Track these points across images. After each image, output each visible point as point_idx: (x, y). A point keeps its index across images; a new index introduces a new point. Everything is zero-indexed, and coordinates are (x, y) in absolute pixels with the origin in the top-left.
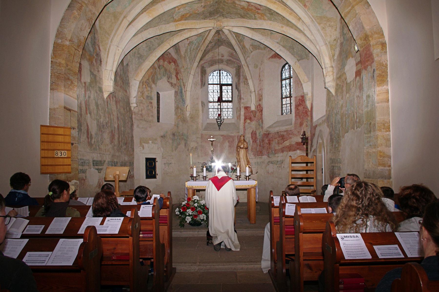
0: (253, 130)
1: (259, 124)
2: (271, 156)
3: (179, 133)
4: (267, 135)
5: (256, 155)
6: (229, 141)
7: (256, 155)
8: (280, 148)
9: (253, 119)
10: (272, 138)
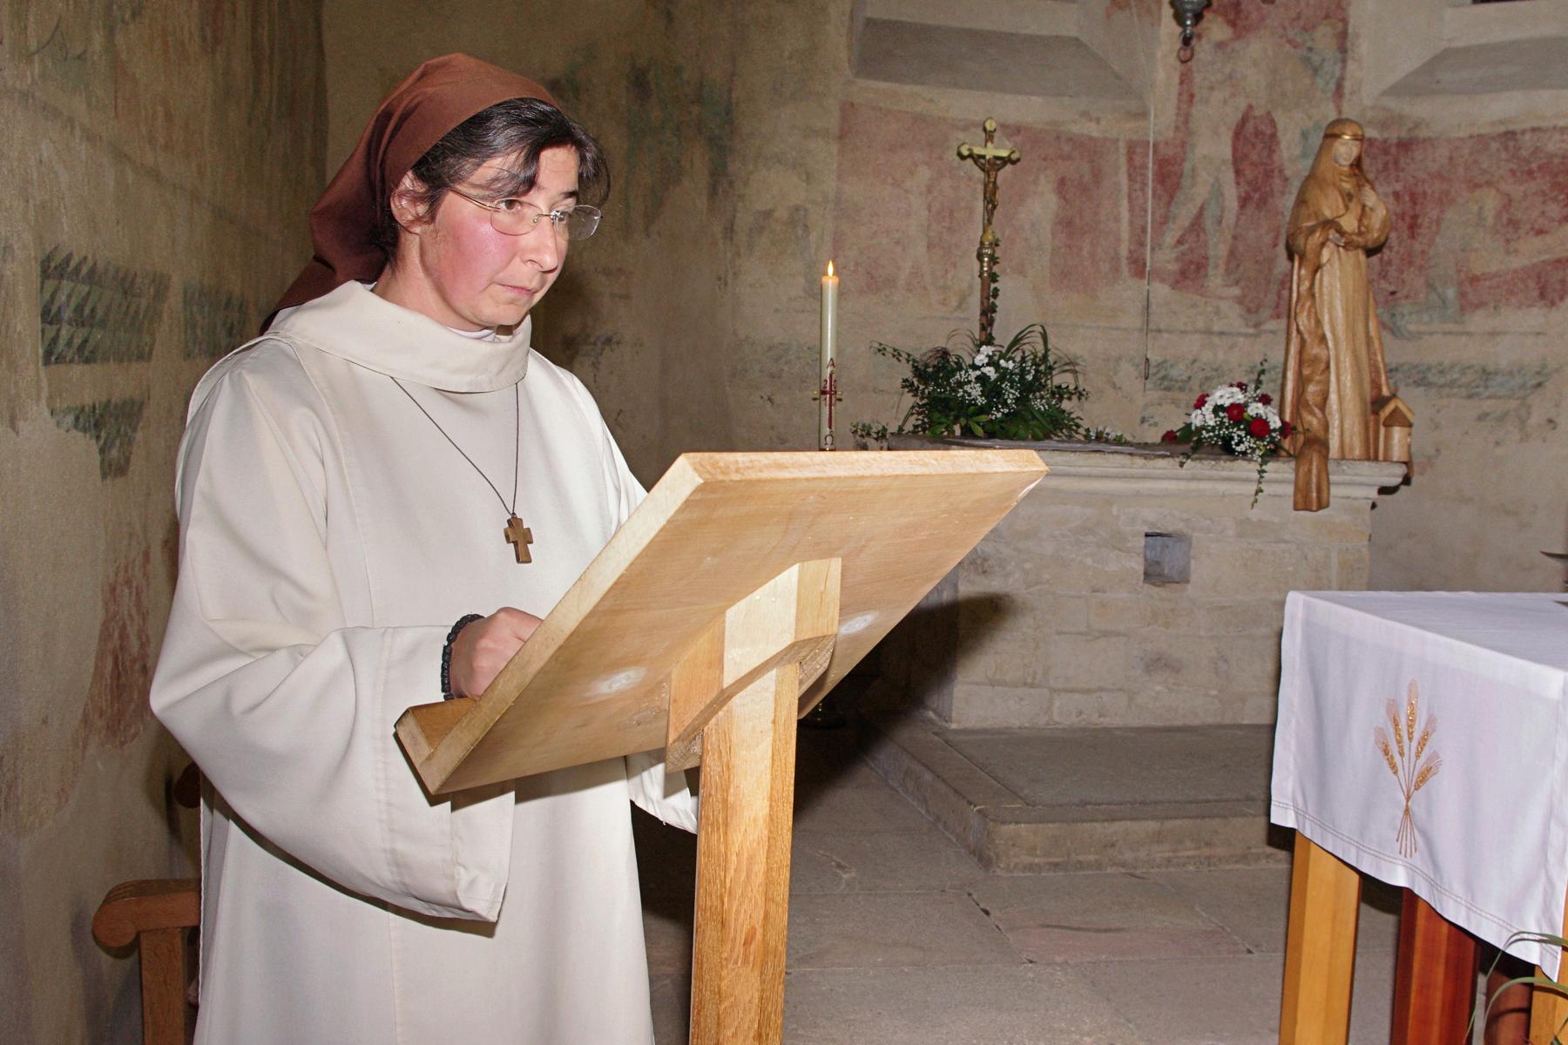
0: (1250, 107)
1: (1306, 61)
2: (1412, 327)
3: (678, 71)
4: (1386, 152)
5: (1266, 312)
6: (1062, 182)
7: (1266, 312)
8: (1517, 263)
9: (1254, 16)
10: (1439, 175)
